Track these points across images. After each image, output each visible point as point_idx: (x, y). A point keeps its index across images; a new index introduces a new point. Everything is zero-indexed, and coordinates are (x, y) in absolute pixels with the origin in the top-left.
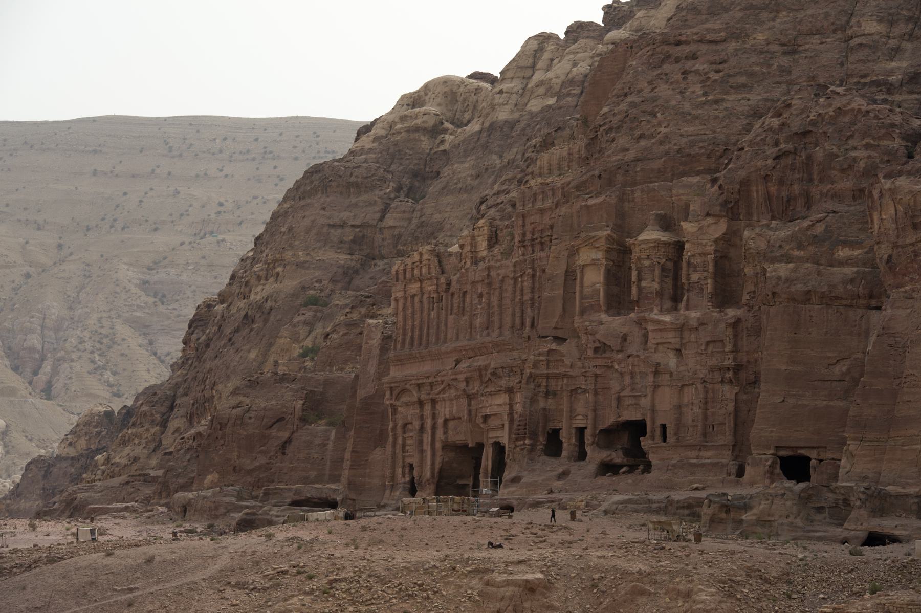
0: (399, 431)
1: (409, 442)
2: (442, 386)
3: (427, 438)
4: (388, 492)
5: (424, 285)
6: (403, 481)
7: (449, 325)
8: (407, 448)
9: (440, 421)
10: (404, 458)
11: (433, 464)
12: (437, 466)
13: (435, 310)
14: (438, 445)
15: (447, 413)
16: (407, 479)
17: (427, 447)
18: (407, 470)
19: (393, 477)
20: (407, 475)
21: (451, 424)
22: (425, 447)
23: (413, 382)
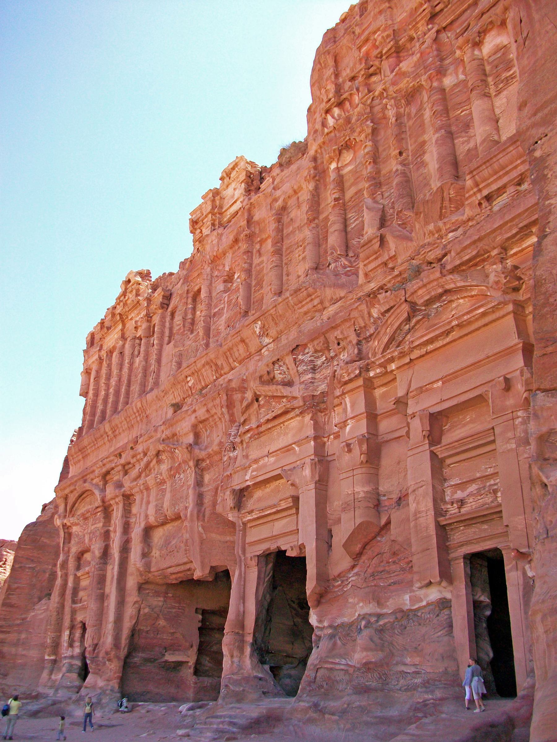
0: (71, 564)
1: (84, 583)
2: (143, 464)
3: (113, 570)
4: (45, 674)
5: (127, 326)
6: (69, 653)
7: (164, 360)
8: (81, 594)
9: (136, 533)
10: (74, 612)
11: (119, 620)
12: (127, 625)
13: (142, 355)
14: (131, 582)
15: (151, 511)
16: (77, 651)
17: (111, 589)
18: (78, 634)
19: (56, 647)
20: (77, 644)
21: (158, 535)
22: (107, 590)
23: (97, 472)
